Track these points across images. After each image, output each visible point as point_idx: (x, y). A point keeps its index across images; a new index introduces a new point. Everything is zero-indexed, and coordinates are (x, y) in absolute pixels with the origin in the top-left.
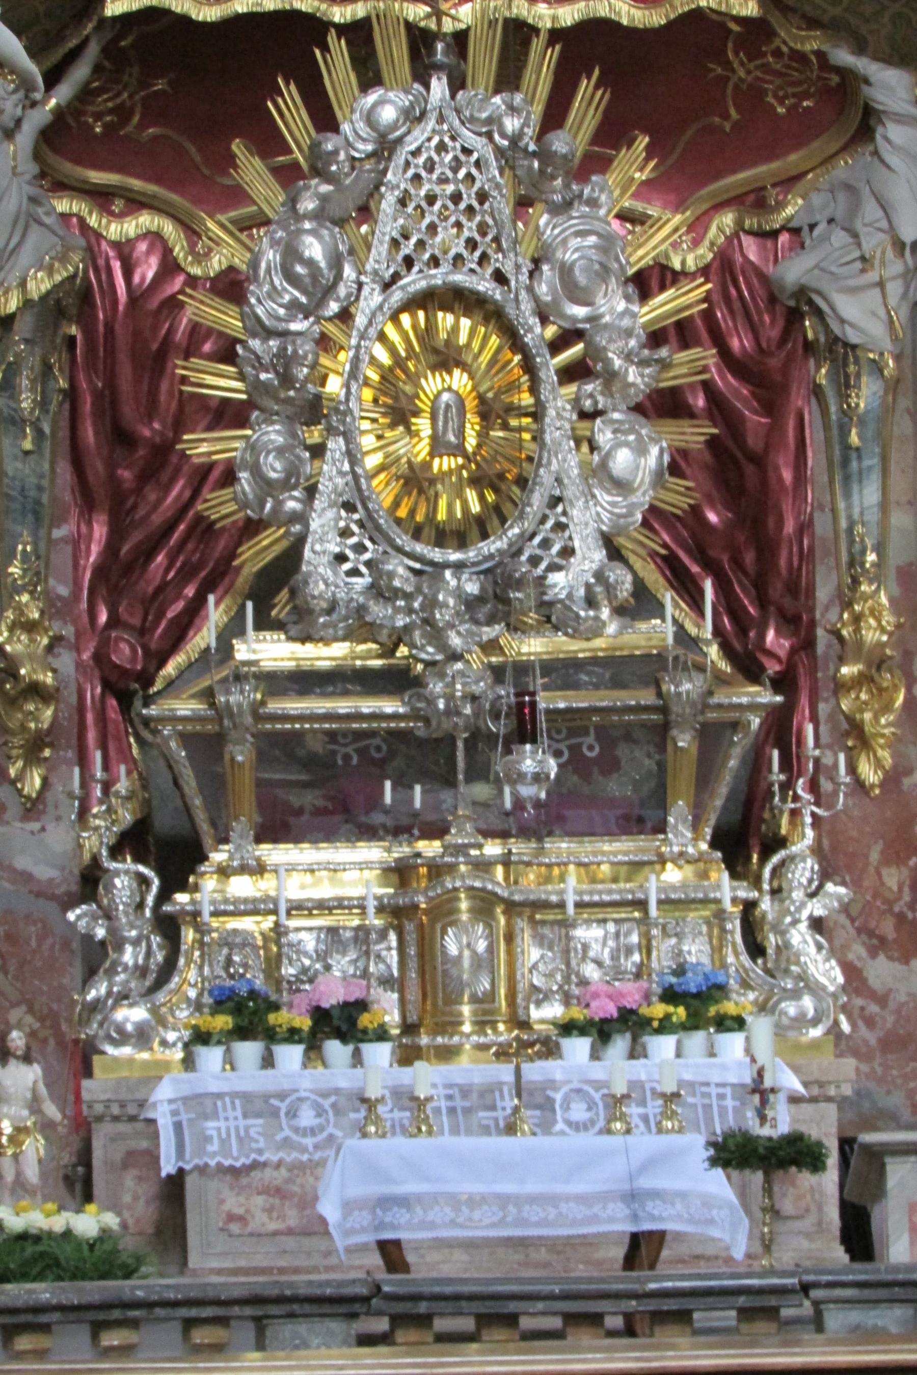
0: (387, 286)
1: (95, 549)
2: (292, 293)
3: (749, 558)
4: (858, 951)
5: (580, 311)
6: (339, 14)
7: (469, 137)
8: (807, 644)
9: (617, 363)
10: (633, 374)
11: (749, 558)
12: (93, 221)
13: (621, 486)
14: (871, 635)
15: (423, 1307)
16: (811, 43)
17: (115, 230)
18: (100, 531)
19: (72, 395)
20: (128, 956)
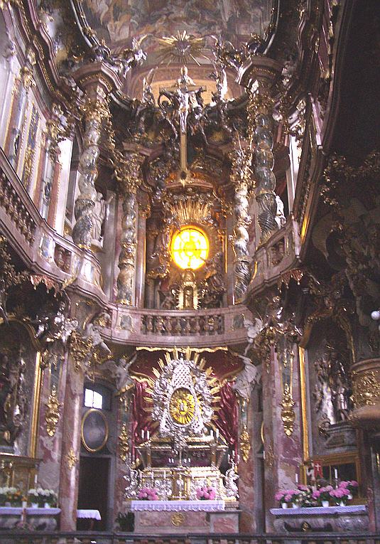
0: (173, 387)
1: (136, 426)
2: (160, 389)
3: (230, 428)
4: (243, 486)
5: (201, 392)
6: (170, 350)
7: (185, 366)
8: (237, 441)
9: (206, 399)
10: (209, 400)
11: (230, 428)
12: (138, 379)
13: (207, 417)
14: (245, 439)
15: (123, 538)
16: (236, 354)
17: (140, 381)
18: (137, 423)
19: (133, 404)
20: (132, 483)
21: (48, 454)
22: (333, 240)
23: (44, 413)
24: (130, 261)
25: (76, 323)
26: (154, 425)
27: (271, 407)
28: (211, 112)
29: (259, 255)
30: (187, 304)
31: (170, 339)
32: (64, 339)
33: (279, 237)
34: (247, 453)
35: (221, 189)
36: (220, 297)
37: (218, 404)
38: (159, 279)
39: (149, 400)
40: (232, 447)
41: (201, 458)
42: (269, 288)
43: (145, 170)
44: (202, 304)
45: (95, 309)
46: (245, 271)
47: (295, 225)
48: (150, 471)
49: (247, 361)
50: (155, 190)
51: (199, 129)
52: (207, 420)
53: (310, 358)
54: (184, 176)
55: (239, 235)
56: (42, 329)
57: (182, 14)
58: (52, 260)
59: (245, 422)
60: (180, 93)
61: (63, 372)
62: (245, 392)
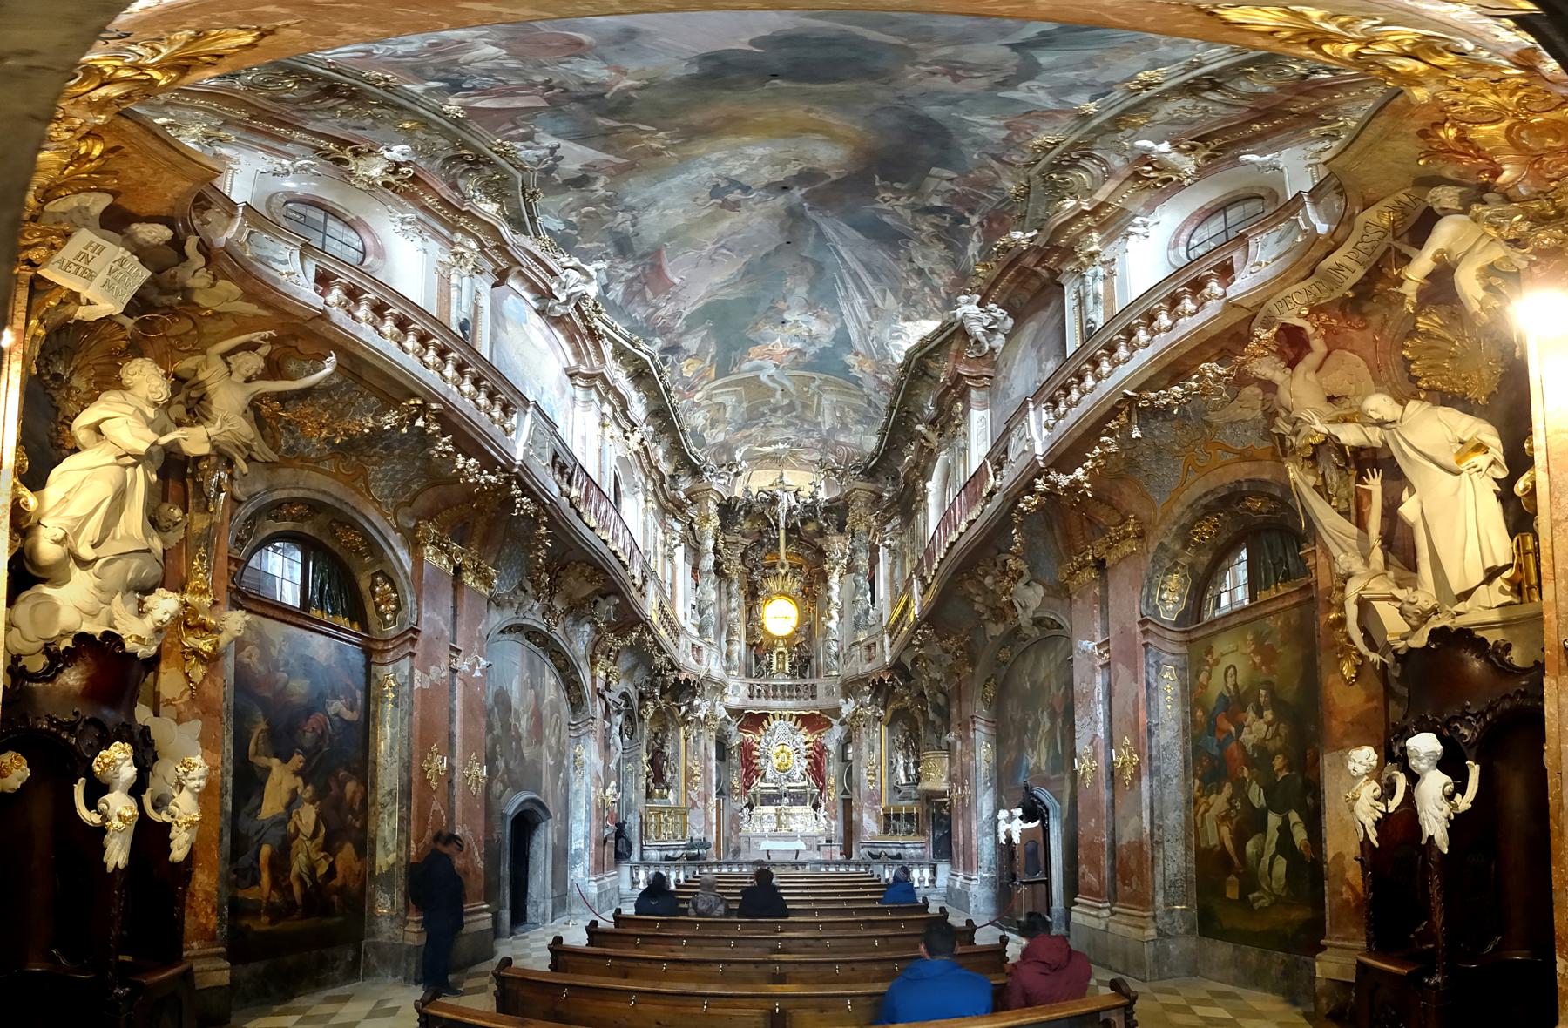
21: (694, 804)
22: (915, 661)
23: (690, 775)
24: (736, 638)
25: (709, 703)
26: (761, 773)
27: (859, 768)
28: (805, 506)
29: (854, 649)
30: (780, 666)
31: (773, 703)
32: (702, 717)
33: (873, 641)
34: (833, 794)
35: (813, 571)
36: (808, 660)
37: (810, 757)
38: (755, 644)
39: (757, 754)
40: (821, 789)
41: (798, 799)
42: (864, 680)
43: (744, 556)
44: (792, 667)
45: (719, 688)
46: (834, 648)
47: (887, 641)
48: (759, 810)
49: (834, 721)
50: (752, 571)
51: (796, 523)
52: (801, 769)
53: (891, 733)
54: (783, 566)
55: (831, 618)
56: (683, 709)
57: (781, 422)
58: (691, 659)
59: (832, 769)
60: (779, 493)
61: (702, 742)
62: (832, 746)
